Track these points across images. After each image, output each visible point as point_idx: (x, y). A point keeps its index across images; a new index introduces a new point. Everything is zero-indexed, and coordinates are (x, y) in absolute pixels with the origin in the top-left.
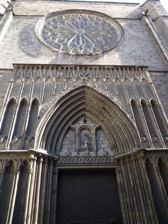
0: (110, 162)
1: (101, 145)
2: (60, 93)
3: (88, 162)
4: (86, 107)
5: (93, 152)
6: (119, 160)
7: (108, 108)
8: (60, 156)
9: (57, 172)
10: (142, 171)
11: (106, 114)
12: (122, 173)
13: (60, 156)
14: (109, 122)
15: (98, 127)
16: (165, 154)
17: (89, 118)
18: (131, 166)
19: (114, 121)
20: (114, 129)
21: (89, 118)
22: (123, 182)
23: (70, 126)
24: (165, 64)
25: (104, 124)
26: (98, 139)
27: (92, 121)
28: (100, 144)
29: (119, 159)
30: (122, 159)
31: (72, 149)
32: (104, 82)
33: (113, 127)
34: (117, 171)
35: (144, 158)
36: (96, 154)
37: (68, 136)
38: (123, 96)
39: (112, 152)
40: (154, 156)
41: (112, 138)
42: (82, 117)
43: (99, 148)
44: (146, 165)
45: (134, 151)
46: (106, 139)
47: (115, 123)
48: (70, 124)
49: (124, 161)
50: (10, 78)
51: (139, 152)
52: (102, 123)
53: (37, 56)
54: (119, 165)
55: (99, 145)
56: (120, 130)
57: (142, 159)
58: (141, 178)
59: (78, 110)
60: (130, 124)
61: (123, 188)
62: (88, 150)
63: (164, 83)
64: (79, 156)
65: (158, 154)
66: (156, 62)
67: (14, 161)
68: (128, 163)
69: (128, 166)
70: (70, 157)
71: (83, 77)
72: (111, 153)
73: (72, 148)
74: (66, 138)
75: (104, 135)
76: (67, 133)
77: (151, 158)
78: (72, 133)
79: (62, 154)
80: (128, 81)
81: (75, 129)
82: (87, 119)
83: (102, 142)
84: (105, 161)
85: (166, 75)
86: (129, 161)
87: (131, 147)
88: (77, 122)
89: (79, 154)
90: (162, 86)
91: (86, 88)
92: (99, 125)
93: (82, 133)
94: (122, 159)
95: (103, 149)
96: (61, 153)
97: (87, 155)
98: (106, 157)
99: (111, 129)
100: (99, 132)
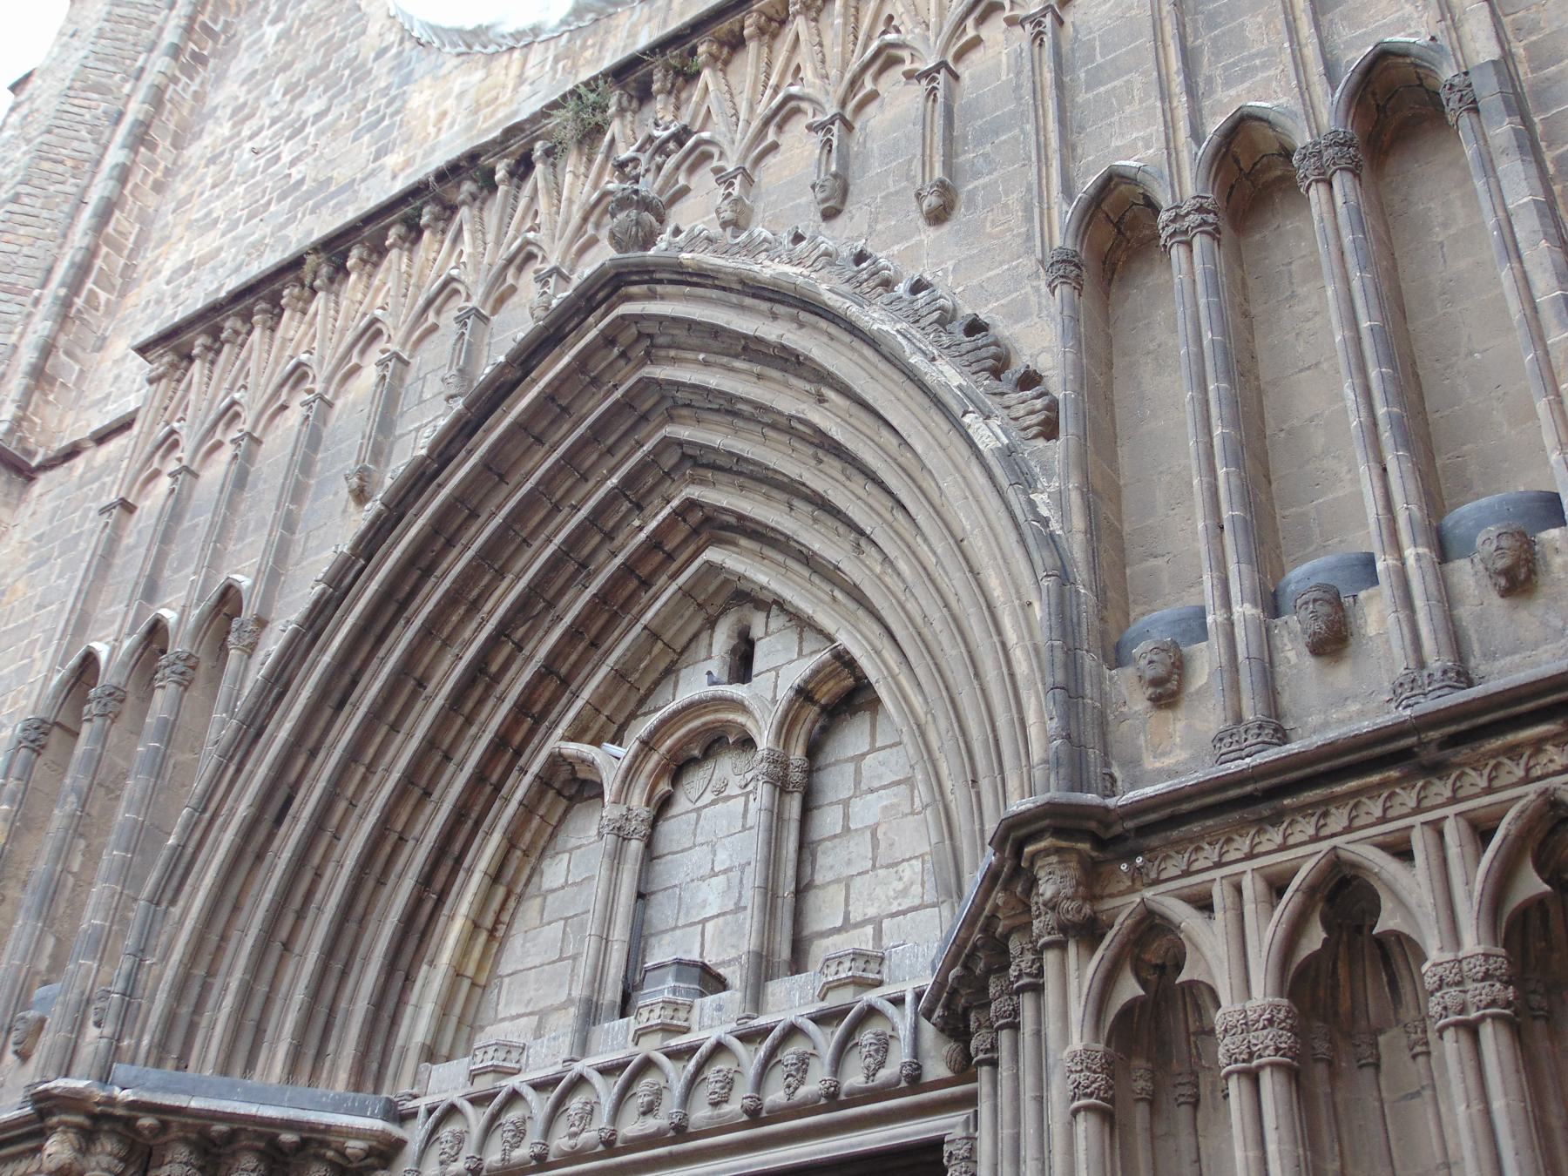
3: (652, 1124)
13: (413, 1115)
26: (828, 821)
28: (847, 882)
35: (1089, 932)
37: (555, 872)
42: (711, 623)
48: (557, 742)
53: (372, 174)
65: (1306, 828)
74: (537, 902)
91: (634, 289)
97: (652, 1046)
100: (853, 738)
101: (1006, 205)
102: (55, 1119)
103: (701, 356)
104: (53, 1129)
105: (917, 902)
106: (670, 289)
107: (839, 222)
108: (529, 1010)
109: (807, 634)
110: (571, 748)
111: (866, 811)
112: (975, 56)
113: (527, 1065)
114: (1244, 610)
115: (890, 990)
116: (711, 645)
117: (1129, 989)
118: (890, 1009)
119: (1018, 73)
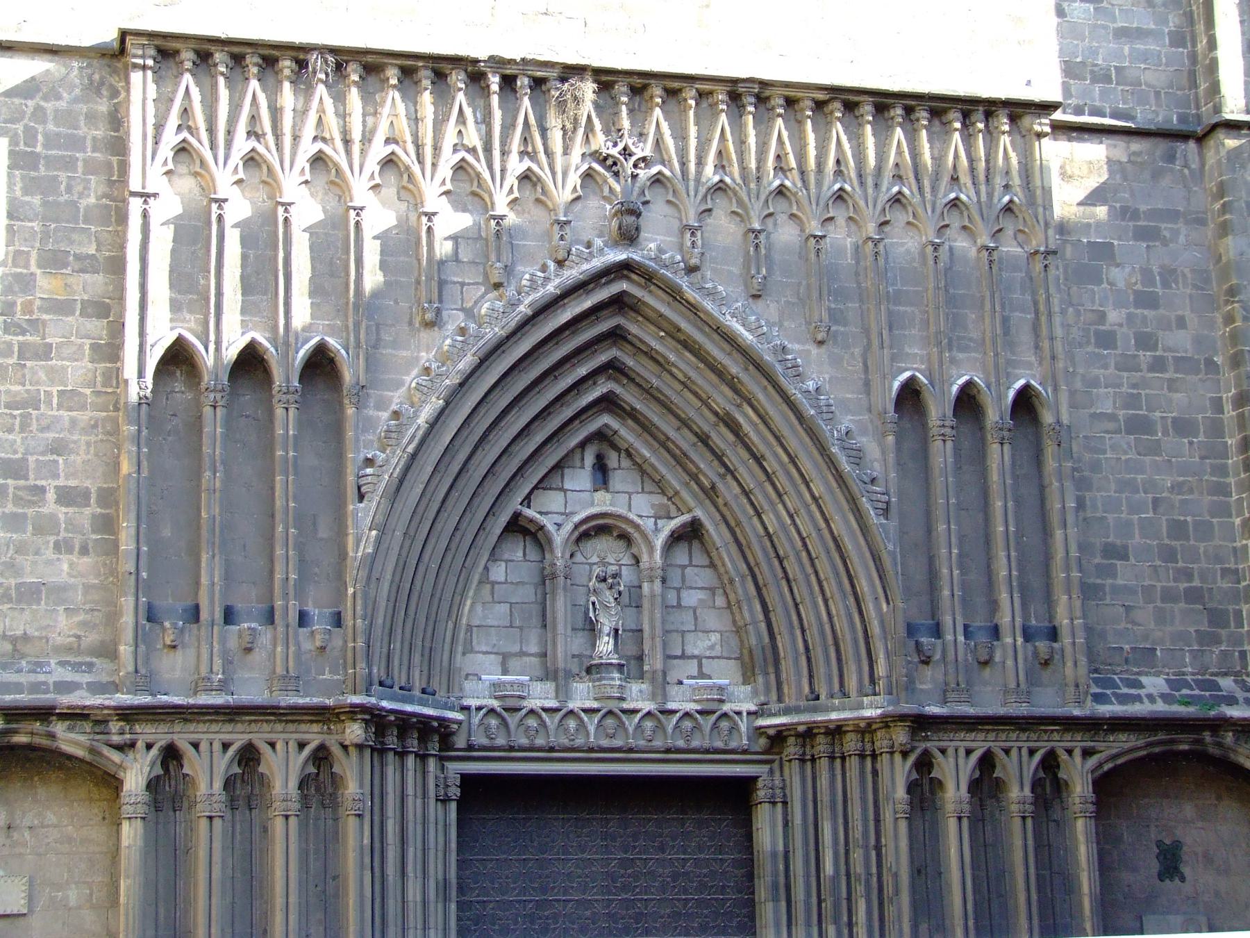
0: (733, 745)
1: (690, 637)
2: (469, 305)
3: (618, 743)
4: (618, 390)
5: (644, 686)
6: (778, 738)
7: (755, 425)
8: (466, 702)
9: (455, 792)
10: (887, 816)
11: (737, 457)
12: (785, 803)
14: (748, 507)
15: (684, 525)
16: (1013, 736)
17: (629, 455)
18: (839, 778)
19: (780, 507)
20: (772, 555)
21: (629, 455)
22: (786, 853)
23: (517, 516)
24: (1194, 44)
25: (718, 510)
27: (643, 473)
29: (779, 733)
30: (798, 735)
31: (527, 659)
32: (753, 231)
33: (768, 544)
34: (761, 793)
35: (905, 754)
36: (659, 699)
37: (498, 572)
38: (857, 351)
39: (749, 688)
40: (959, 741)
41: (758, 607)
43: (676, 657)
44: (912, 788)
45: (868, 713)
46: (720, 601)
47: (782, 524)
48: (514, 504)
49: (804, 746)
50: (99, 133)
51: (887, 722)
52: (707, 502)
54: (776, 765)
55: (676, 638)
56: (810, 570)
57: (898, 757)
58: (878, 848)
59: (568, 413)
60: (868, 555)
61: (782, 880)
62: (616, 675)
63: (1143, 234)
64: (571, 705)
65: (981, 736)
66: (1143, 19)
67: (265, 749)
68: (824, 763)
69: (824, 781)
70: (524, 712)
71: (616, 174)
72: (742, 701)
73: (522, 654)
75: (709, 571)
76: (494, 556)
77: (943, 751)
78: (520, 554)
79: (477, 695)
80: (909, 223)
81: (540, 535)
82: (612, 459)
83: (696, 619)
84: (707, 737)
85: (1171, 158)
86: (833, 752)
87: (852, 683)
88: (555, 481)
89: (563, 692)
90: (1118, 265)
92: (686, 518)
93: (579, 558)
94: (798, 735)
95: (695, 661)
96: (469, 685)
97: (613, 705)
98: (714, 717)
99: (758, 552)
101: (853, 353)
102: (359, 716)
103: (662, 334)
104: (355, 720)
105: (719, 654)
106: (660, 292)
107: (760, 303)
108: (495, 650)
109: (646, 479)
110: (530, 513)
111: (691, 598)
112: (831, 227)
113: (529, 695)
114: (961, 638)
115: (737, 709)
116: (583, 459)
117: (915, 776)
118: (736, 717)
119: (858, 263)
